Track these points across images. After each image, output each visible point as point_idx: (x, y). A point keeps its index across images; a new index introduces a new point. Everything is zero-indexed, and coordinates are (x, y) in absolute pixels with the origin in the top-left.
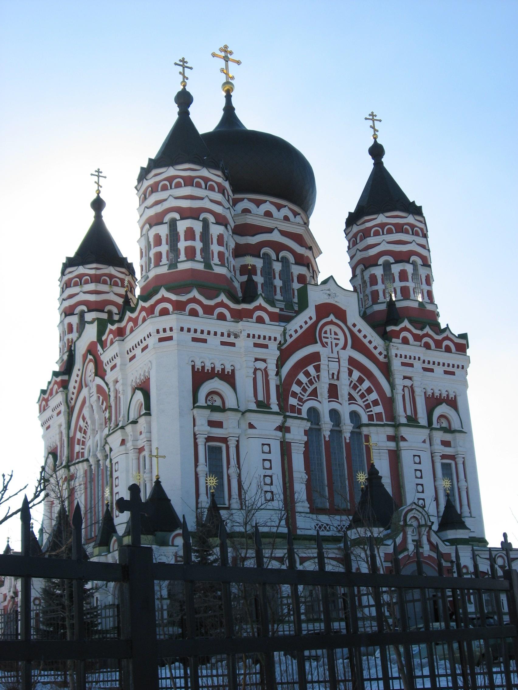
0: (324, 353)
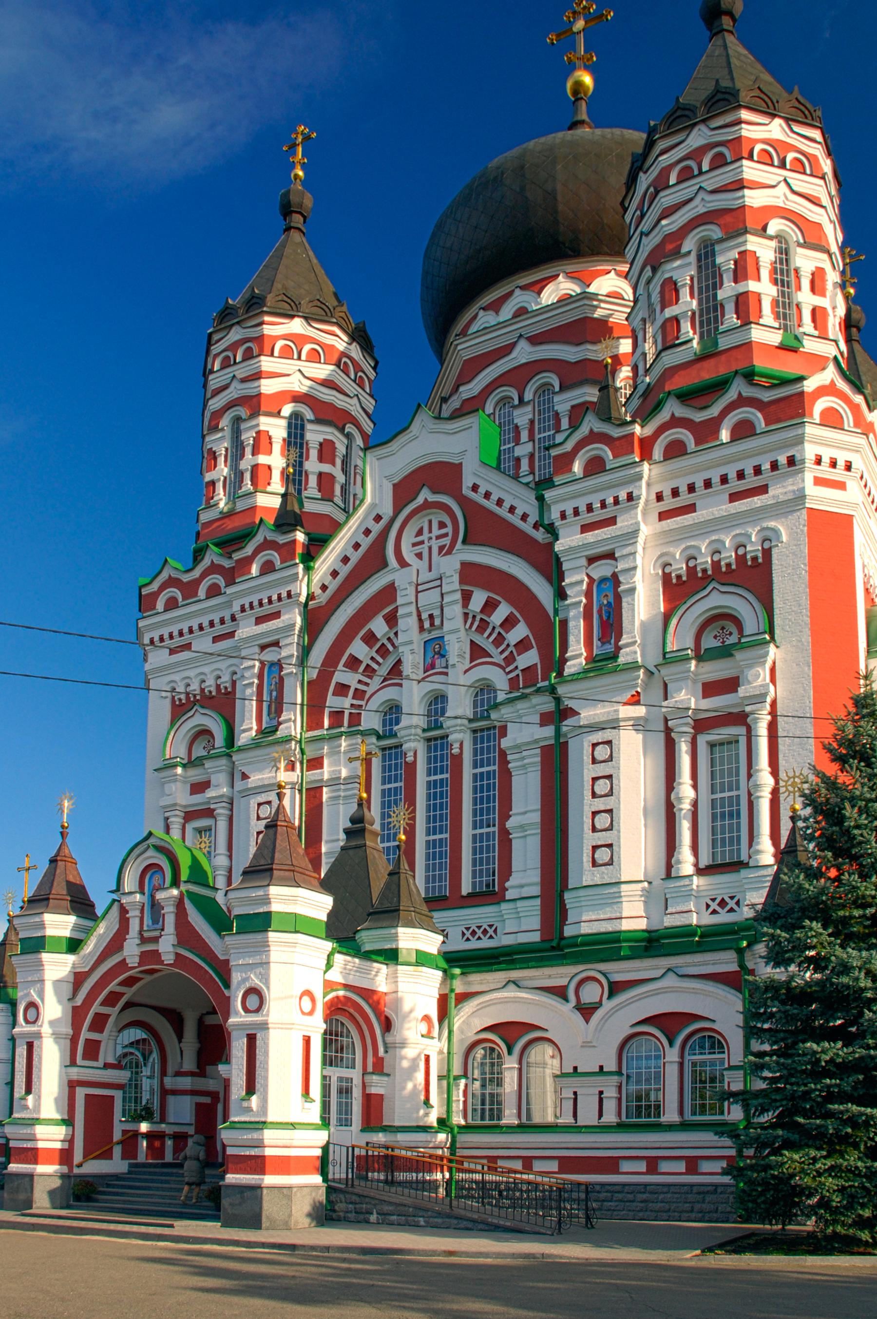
0: (403, 579)
